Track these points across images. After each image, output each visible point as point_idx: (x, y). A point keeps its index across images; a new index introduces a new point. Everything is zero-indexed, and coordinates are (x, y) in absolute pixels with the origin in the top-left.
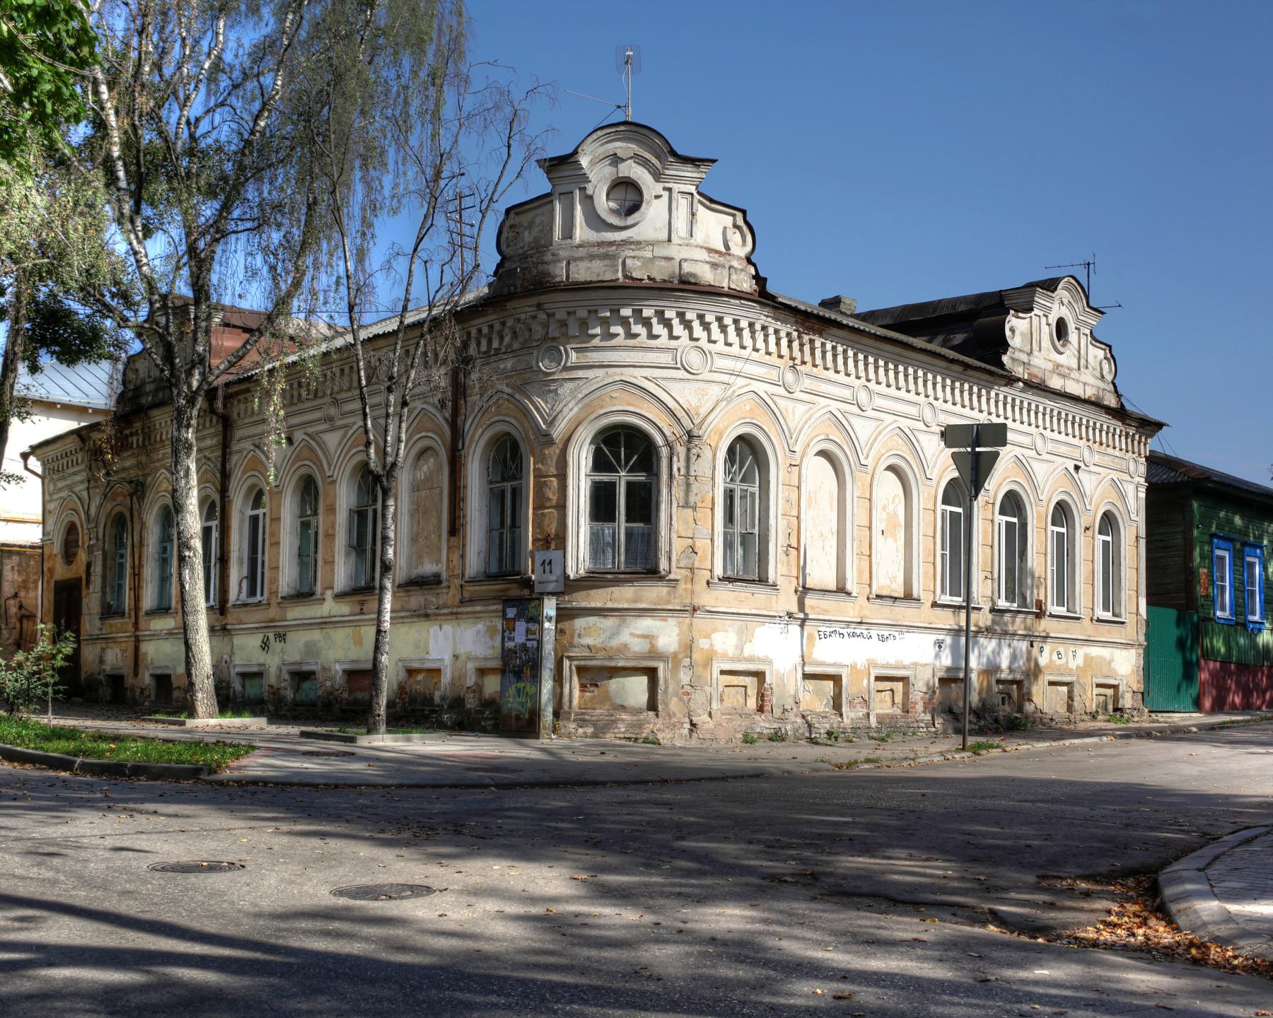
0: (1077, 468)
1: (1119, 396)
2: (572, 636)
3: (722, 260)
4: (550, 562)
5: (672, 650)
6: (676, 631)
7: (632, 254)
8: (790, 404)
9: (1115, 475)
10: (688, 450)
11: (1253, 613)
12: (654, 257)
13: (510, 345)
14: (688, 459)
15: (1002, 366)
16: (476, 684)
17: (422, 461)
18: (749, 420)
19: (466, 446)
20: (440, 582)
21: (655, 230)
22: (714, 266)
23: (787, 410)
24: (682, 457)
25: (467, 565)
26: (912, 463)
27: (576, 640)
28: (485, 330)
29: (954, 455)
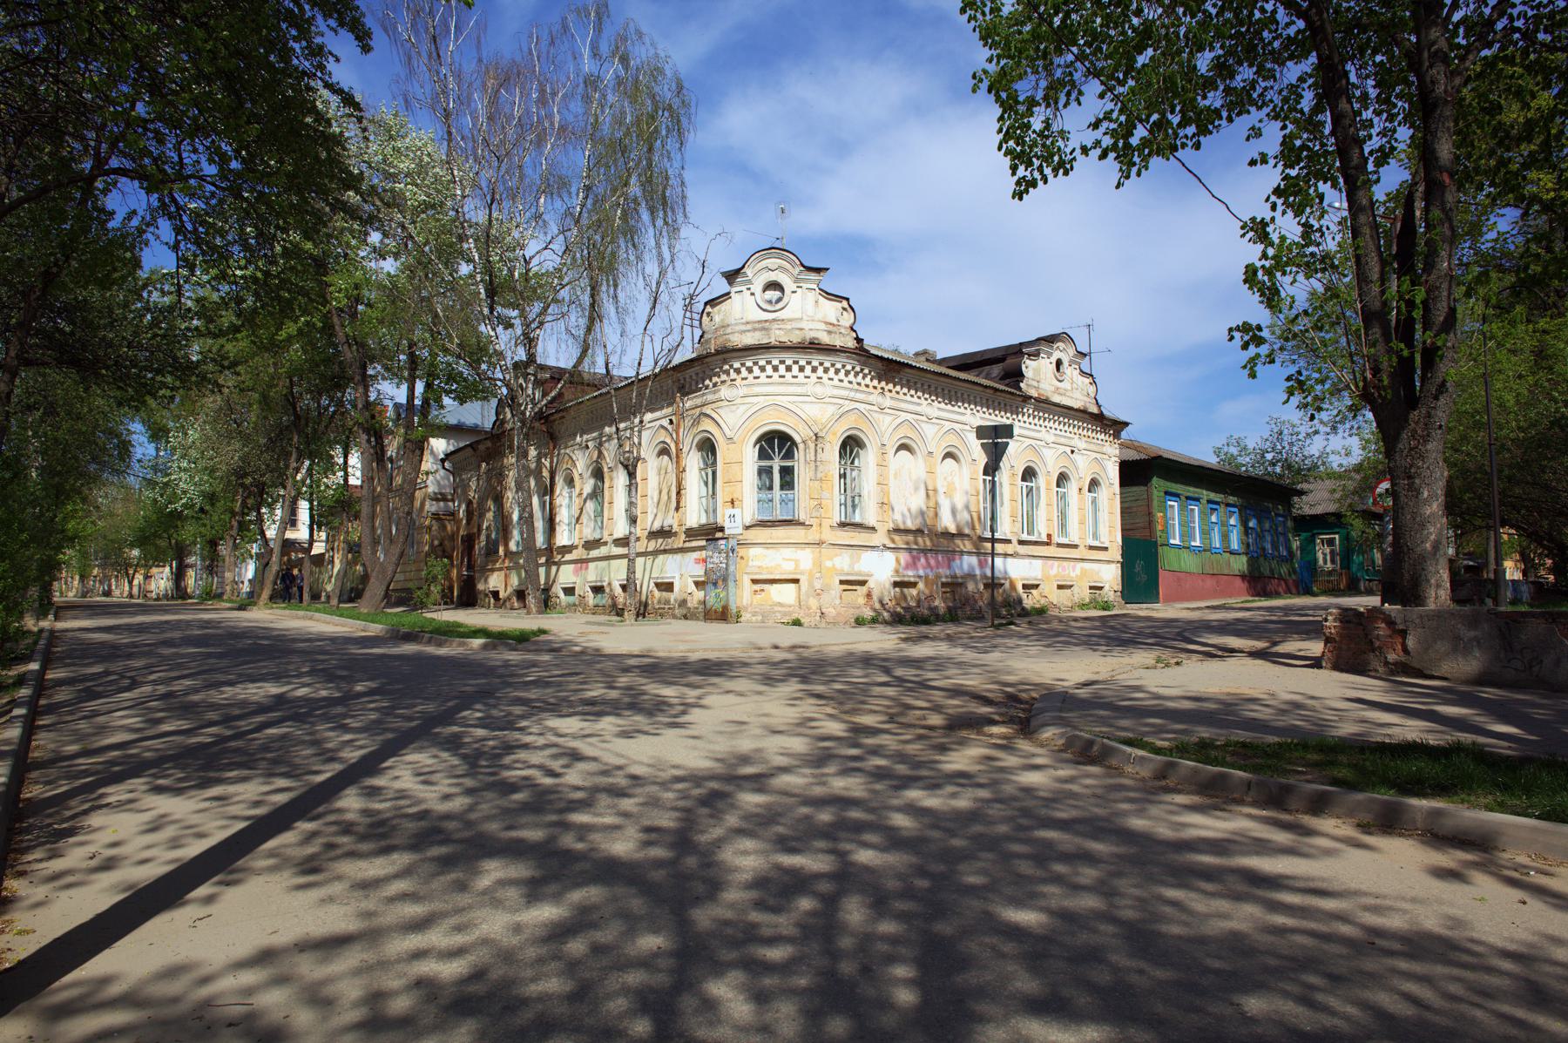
0: (1072, 452)
1: (1099, 407)
3: (835, 329)
8: (881, 416)
9: (1095, 455)
11: (1195, 540)
15: (1020, 389)
22: (830, 332)
27: (750, 563)
29: (982, 444)
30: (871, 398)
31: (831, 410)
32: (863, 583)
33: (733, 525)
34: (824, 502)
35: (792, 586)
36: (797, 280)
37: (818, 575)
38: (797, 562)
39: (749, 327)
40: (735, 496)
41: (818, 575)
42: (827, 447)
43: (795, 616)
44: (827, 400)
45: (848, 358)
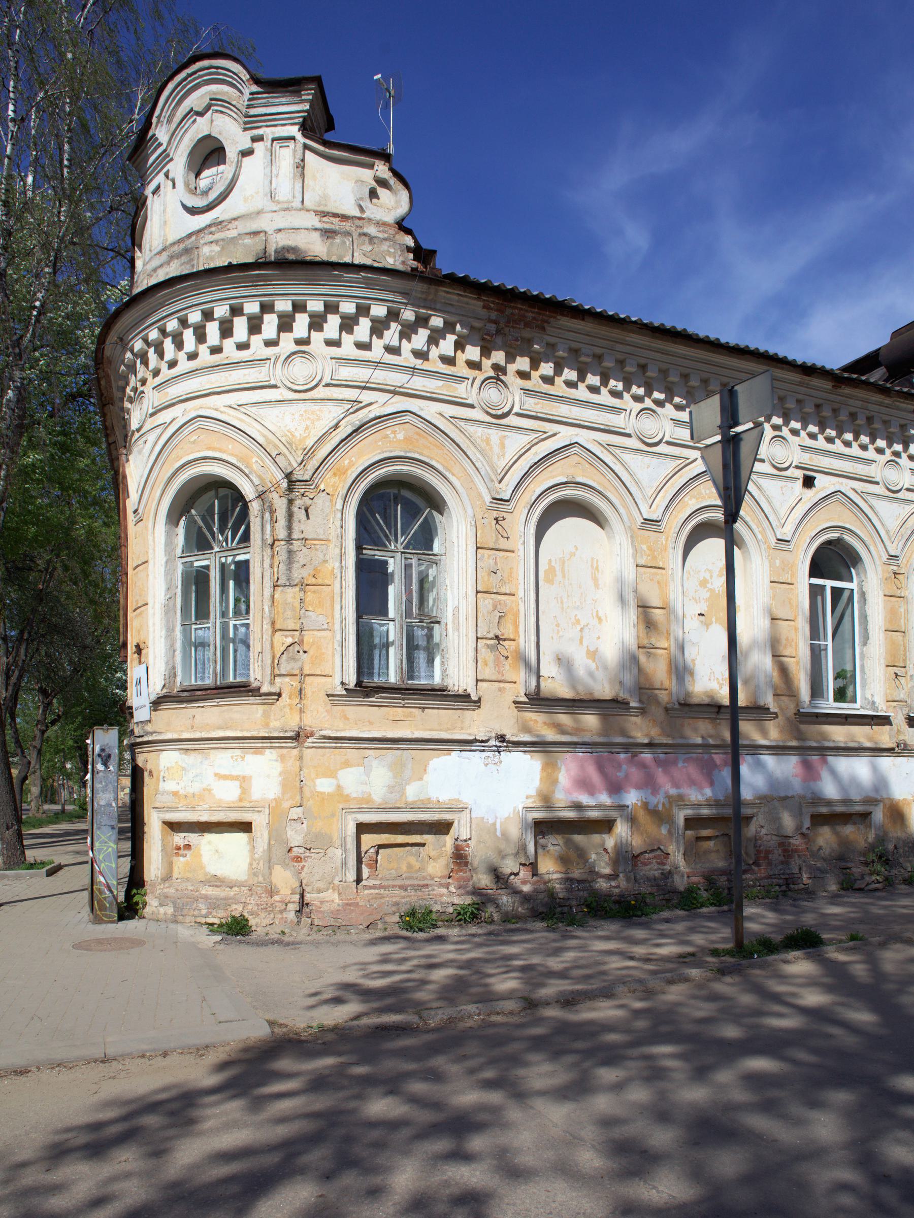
5: (271, 796)
6: (278, 767)
7: (211, 238)
10: (291, 502)
14: (290, 516)
18: (402, 454)
22: (328, 234)
23: (488, 441)
26: (858, 532)
30: (461, 390)
31: (330, 414)
32: (442, 828)
34: (308, 637)
35: (241, 837)
36: (250, 122)
38: (244, 781)
41: (296, 813)
42: (320, 504)
43: (237, 910)
45: (369, 285)
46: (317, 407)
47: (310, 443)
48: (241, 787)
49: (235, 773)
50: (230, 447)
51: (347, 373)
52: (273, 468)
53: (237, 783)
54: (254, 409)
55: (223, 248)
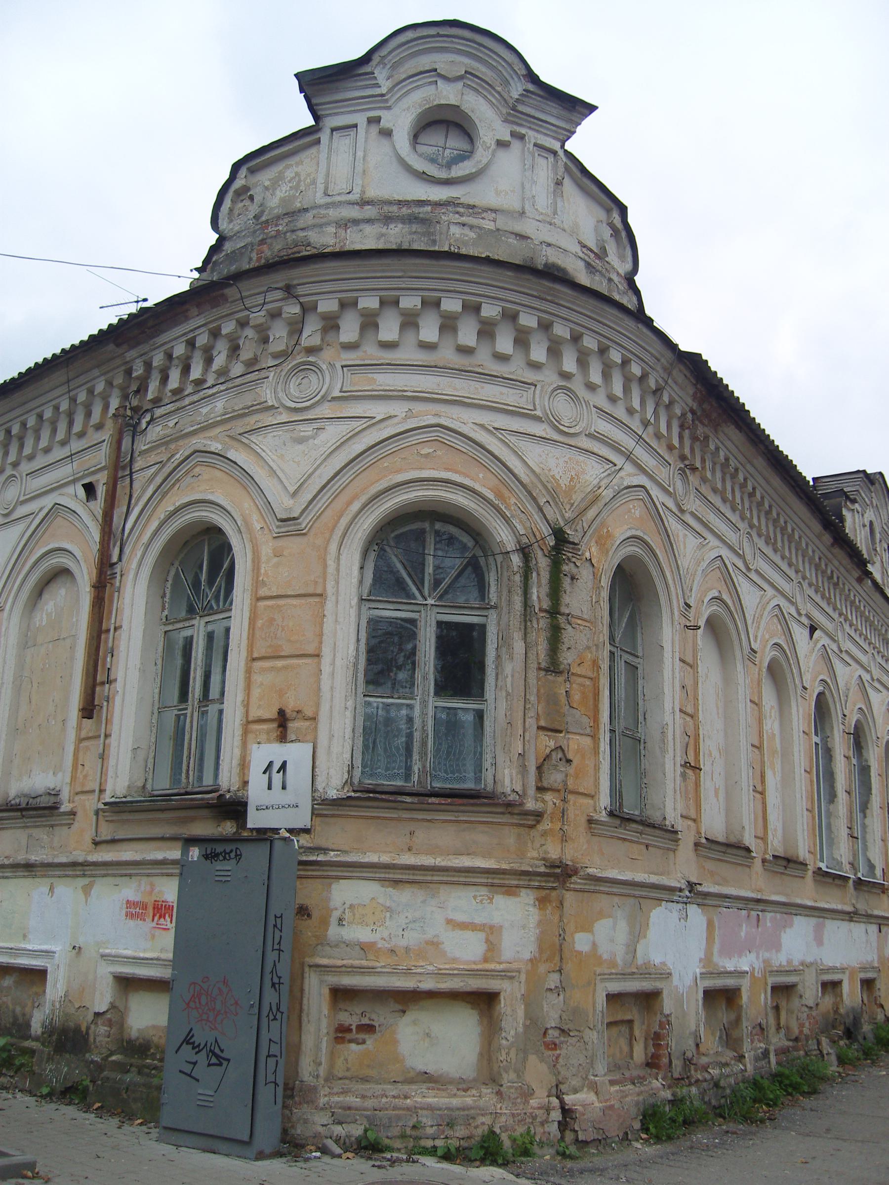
2: (325, 922)
4: (283, 767)
6: (533, 915)
12: (498, 230)
13: (223, 372)
16: (113, 1007)
17: (46, 596)
19: (125, 558)
20: (53, 808)
21: (498, 193)
24: (545, 576)
25: (111, 773)
27: (333, 931)
28: (179, 350)
33: (277, 796)
37: (553, 980)
39: (370, 212)
40: (290, 705)
44: (585, 443)
46: (581, 458)
47: (577, 498)
48: (487, 941)
49: (478, 920)
50: (481, 476)
51: (604, 427)
52: (537, 517)
53: (481, 936)
54: (513, 439)
55: (480, 237)
